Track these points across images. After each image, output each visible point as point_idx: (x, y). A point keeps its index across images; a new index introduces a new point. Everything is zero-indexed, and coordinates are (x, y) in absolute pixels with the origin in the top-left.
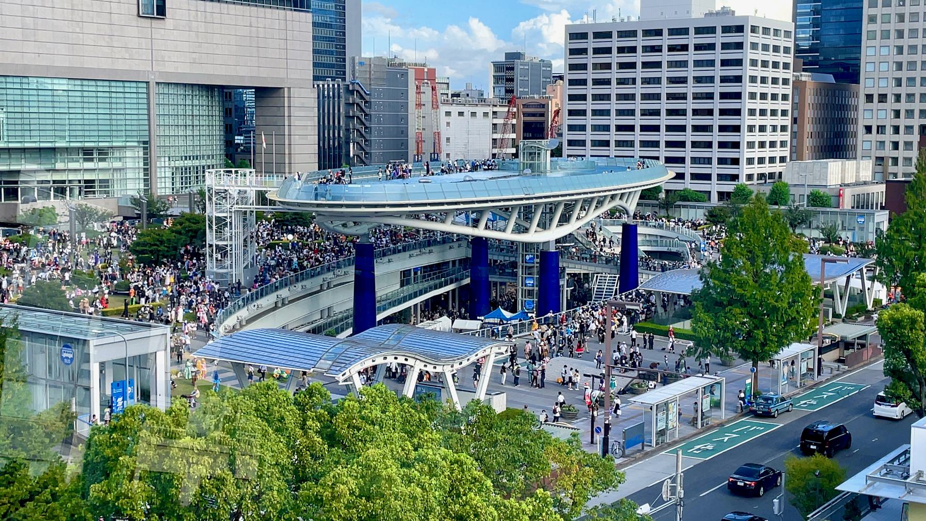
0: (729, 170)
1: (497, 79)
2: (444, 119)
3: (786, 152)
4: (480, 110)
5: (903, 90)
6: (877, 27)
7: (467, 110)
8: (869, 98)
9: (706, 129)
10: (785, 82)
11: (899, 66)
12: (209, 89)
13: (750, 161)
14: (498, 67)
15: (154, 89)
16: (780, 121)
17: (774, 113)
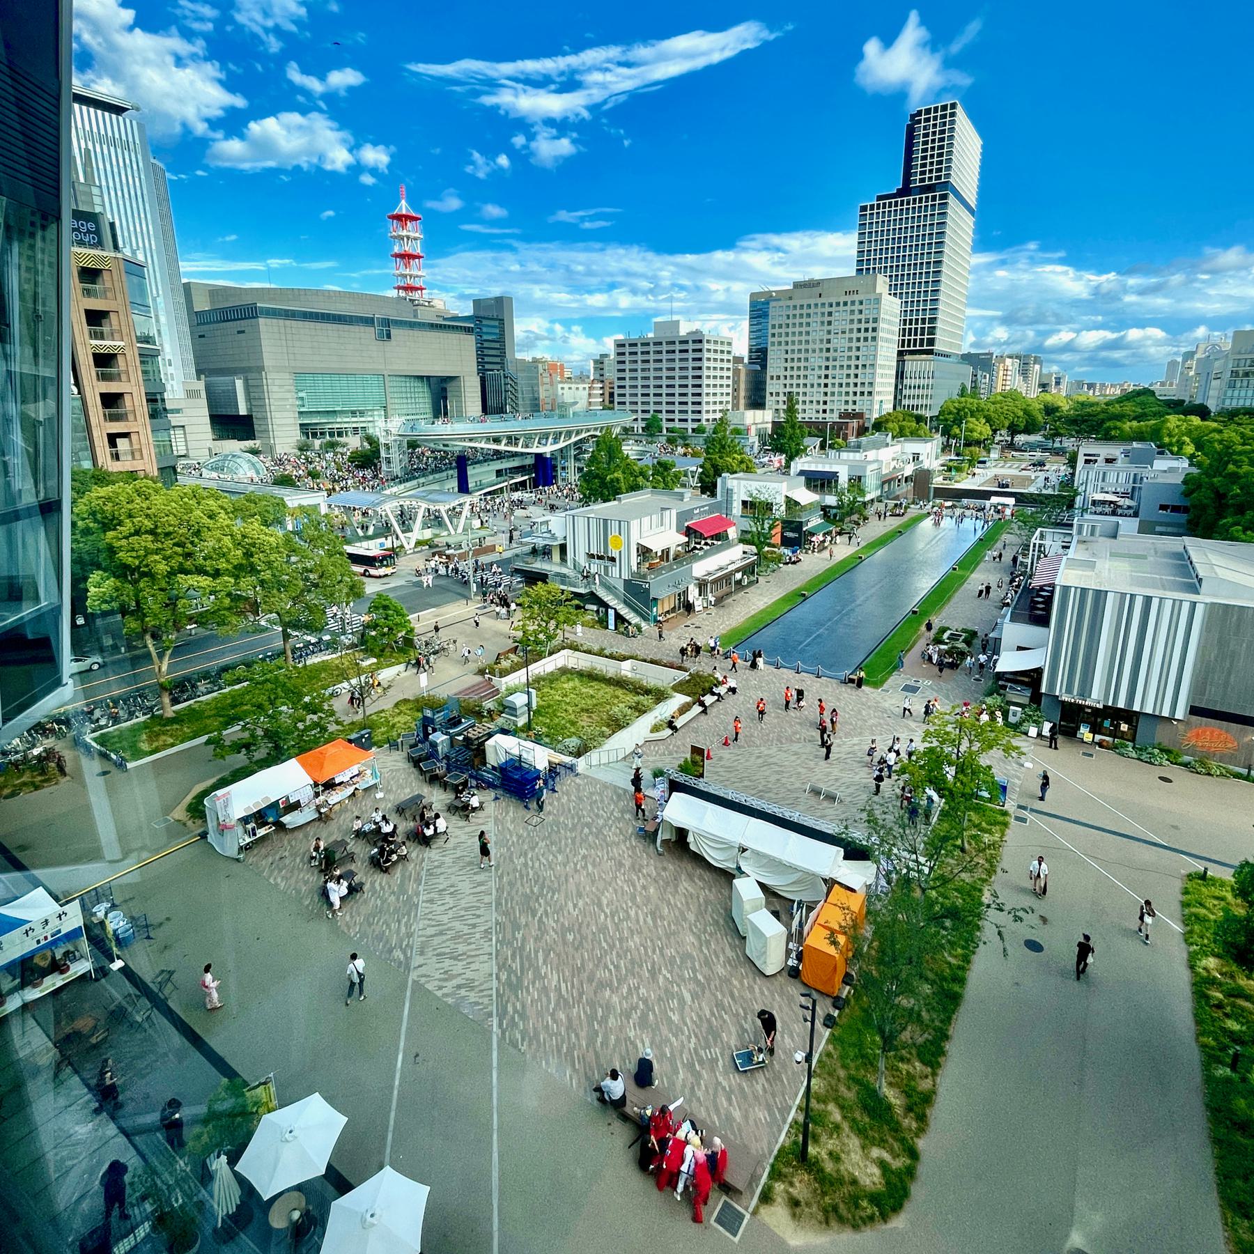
0: (696, 416)
1: (595, 369)
2: (560, 392)
3: (730, 407)
4: (581, 386)
5: (788, 373)
6: (776, 339)
7: (573, 386)
8: (772, 378)
9: (685, 395)
10: (728, 369)
11: (786, 360)
12: (421, 378)
13: (708, 412)
14: (596, 362)
15: (387, 379)
16: (725, 390)
17: (721, 386)
